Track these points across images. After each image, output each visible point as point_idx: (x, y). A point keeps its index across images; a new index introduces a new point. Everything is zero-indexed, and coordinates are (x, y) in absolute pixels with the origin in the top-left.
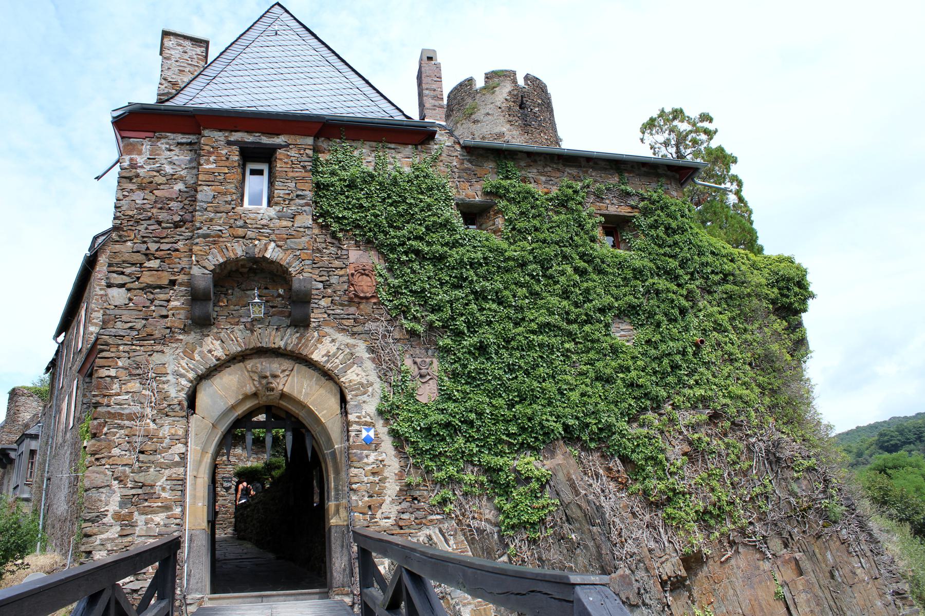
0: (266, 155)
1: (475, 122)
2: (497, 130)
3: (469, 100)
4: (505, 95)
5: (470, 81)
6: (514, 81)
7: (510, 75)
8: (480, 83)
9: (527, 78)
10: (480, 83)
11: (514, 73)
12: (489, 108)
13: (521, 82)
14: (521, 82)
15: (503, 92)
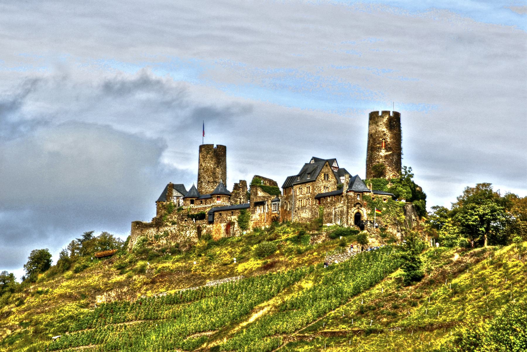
0: (359, 195)
1: (378, 126)
2: (383, 130)
3: (376, 118)
4: (386, 119)
5: (378, 112)
6: (389, 114)
7: (387, 113)
8: (380, 114)
9: (394, 112)
10: (380, 114)
11: (389, 112)
12: (381, 123)
13: (391, 114)
14: (391, 114)
15: (385, 119)
